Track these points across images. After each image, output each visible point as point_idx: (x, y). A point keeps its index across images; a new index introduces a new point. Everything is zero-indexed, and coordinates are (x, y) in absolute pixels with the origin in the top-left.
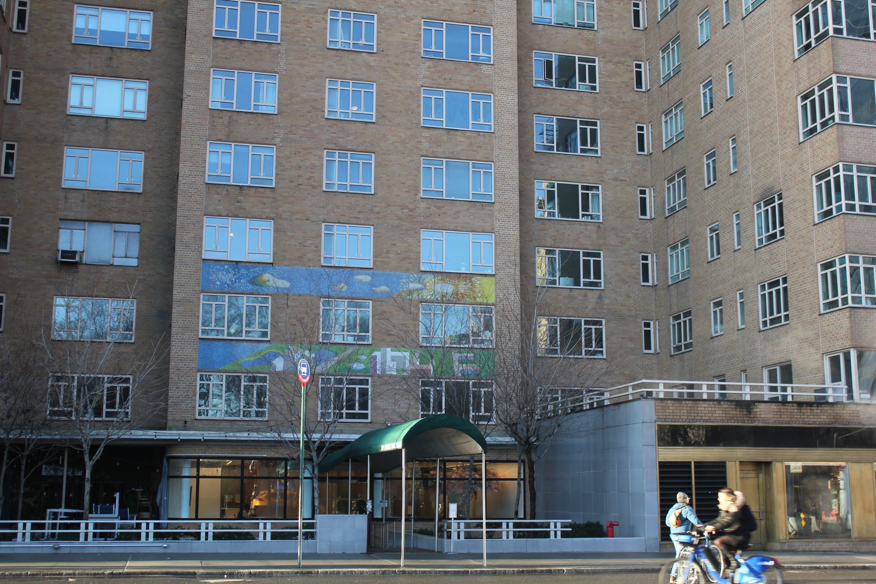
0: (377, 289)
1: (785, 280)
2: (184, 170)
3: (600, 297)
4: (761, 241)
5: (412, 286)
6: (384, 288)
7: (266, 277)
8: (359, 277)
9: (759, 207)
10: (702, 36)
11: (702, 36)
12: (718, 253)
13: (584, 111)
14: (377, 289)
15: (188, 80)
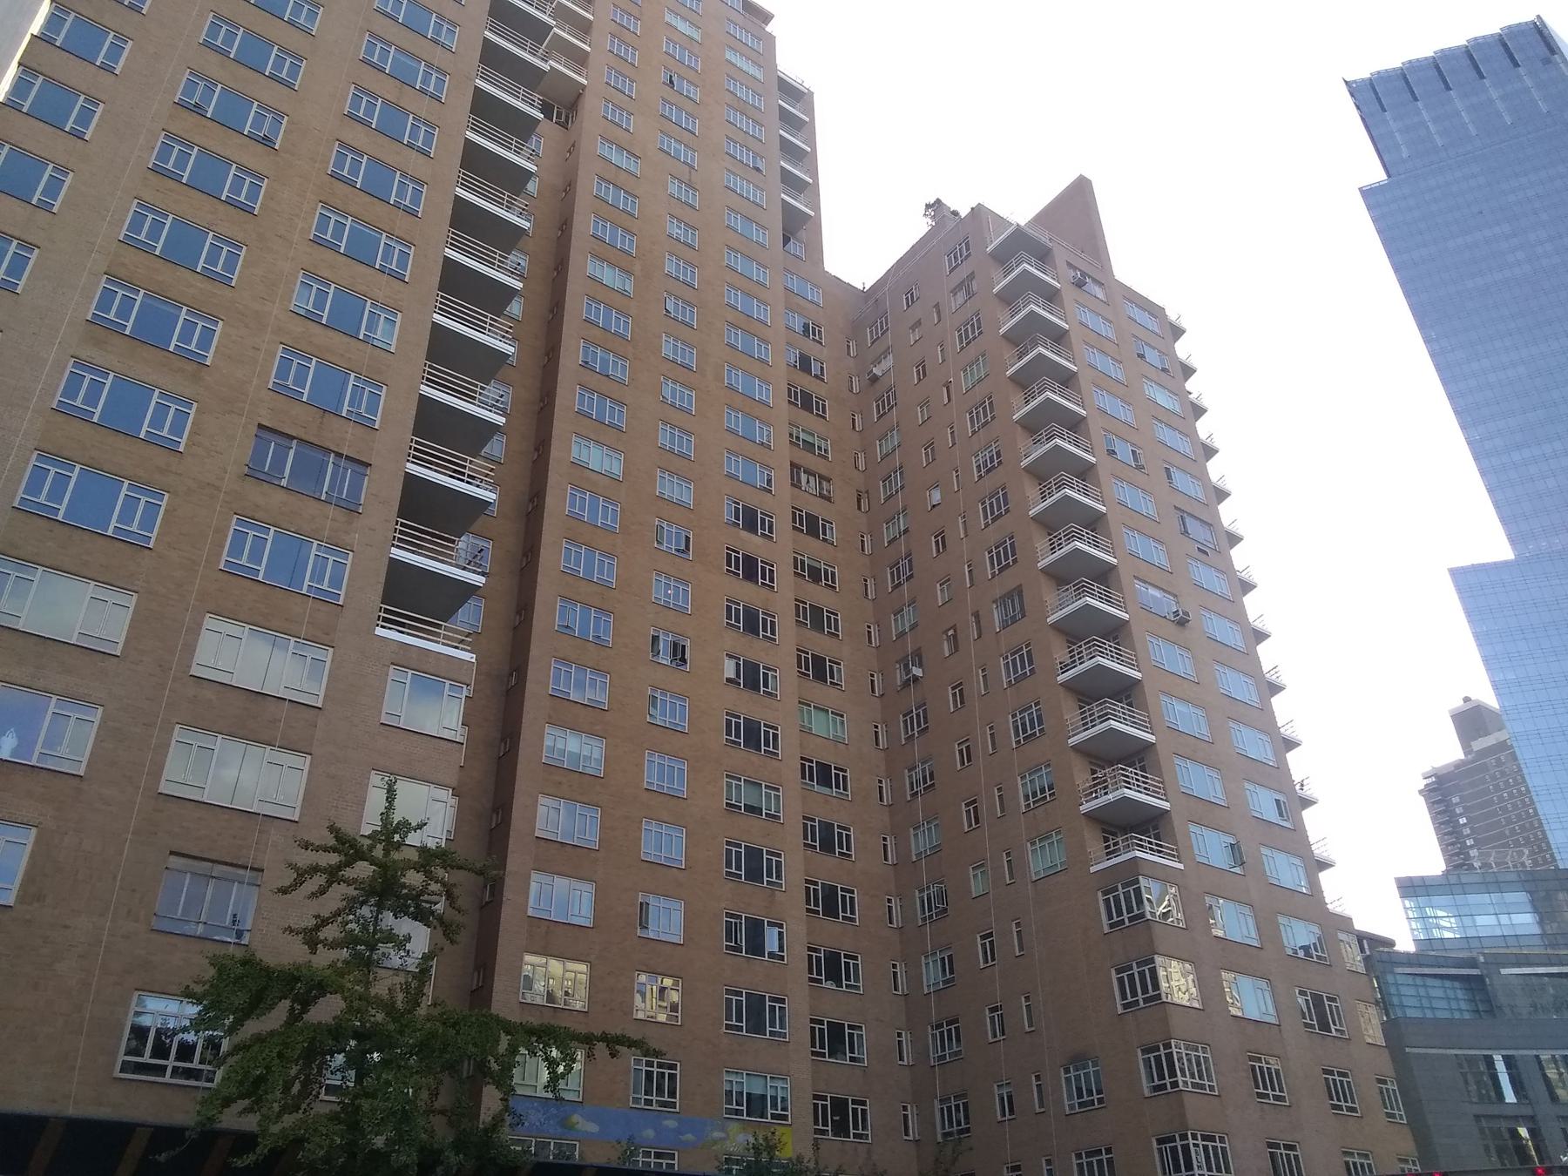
0: (684, 1138)
1: (1109, 1151)
2: (499, 984)
3: (869, 1152)
4: (1072, 1107)
5: (717, 1134)
6: (689, 1137)
7: (576, 1118)
8: (666, 1122)
9: (1067, 1071)
10: (976, 888)
11: (976, 888)
12: (1012, 1111)
13: (844, 946)
14: (684, 1138)
15: (509, 882)
